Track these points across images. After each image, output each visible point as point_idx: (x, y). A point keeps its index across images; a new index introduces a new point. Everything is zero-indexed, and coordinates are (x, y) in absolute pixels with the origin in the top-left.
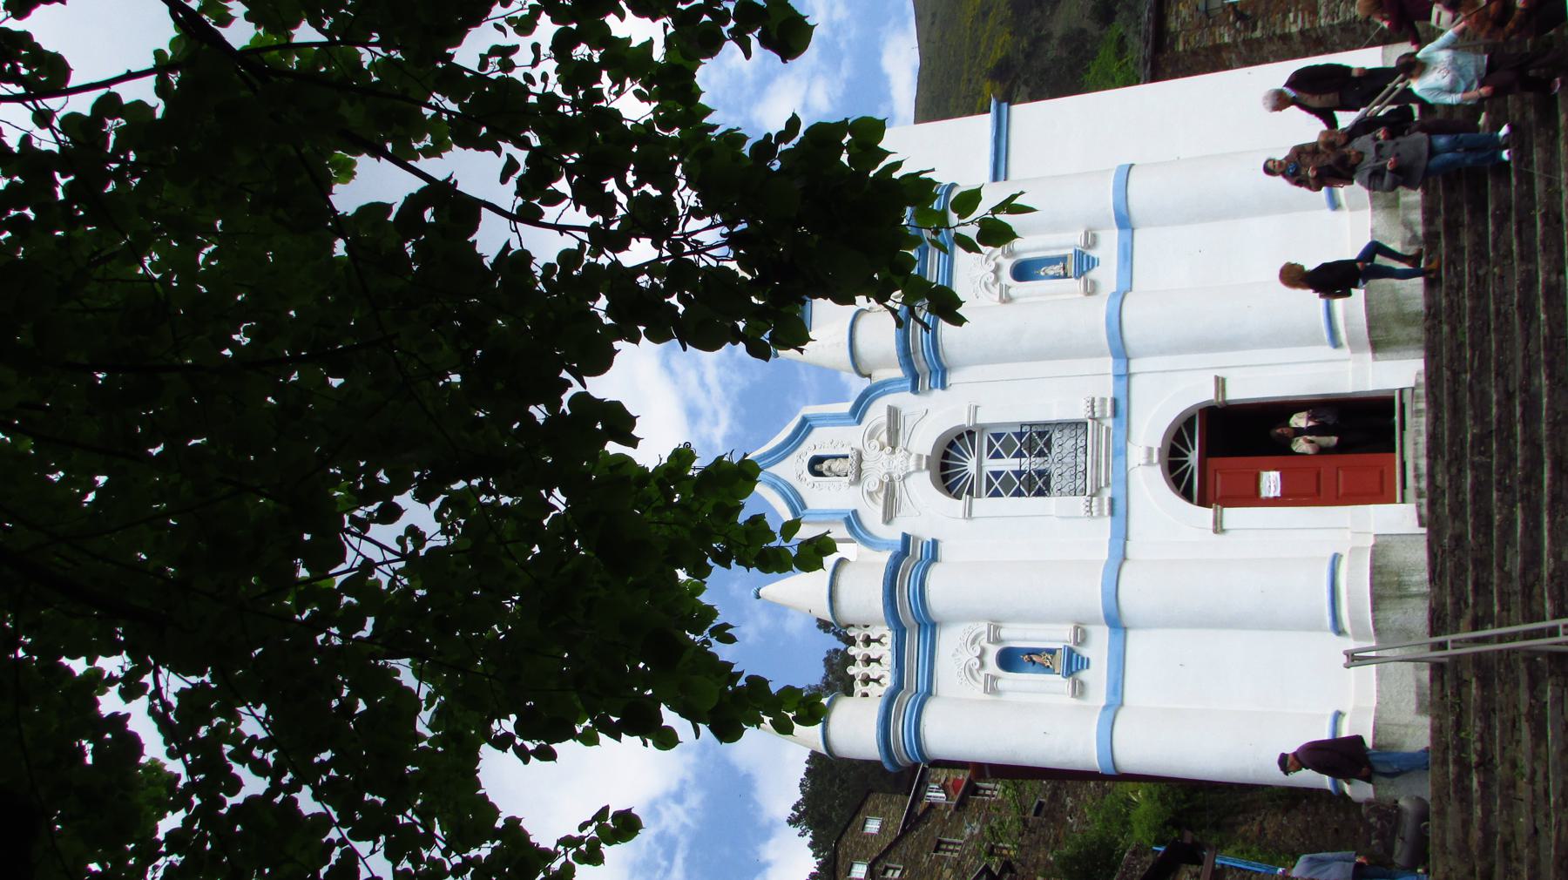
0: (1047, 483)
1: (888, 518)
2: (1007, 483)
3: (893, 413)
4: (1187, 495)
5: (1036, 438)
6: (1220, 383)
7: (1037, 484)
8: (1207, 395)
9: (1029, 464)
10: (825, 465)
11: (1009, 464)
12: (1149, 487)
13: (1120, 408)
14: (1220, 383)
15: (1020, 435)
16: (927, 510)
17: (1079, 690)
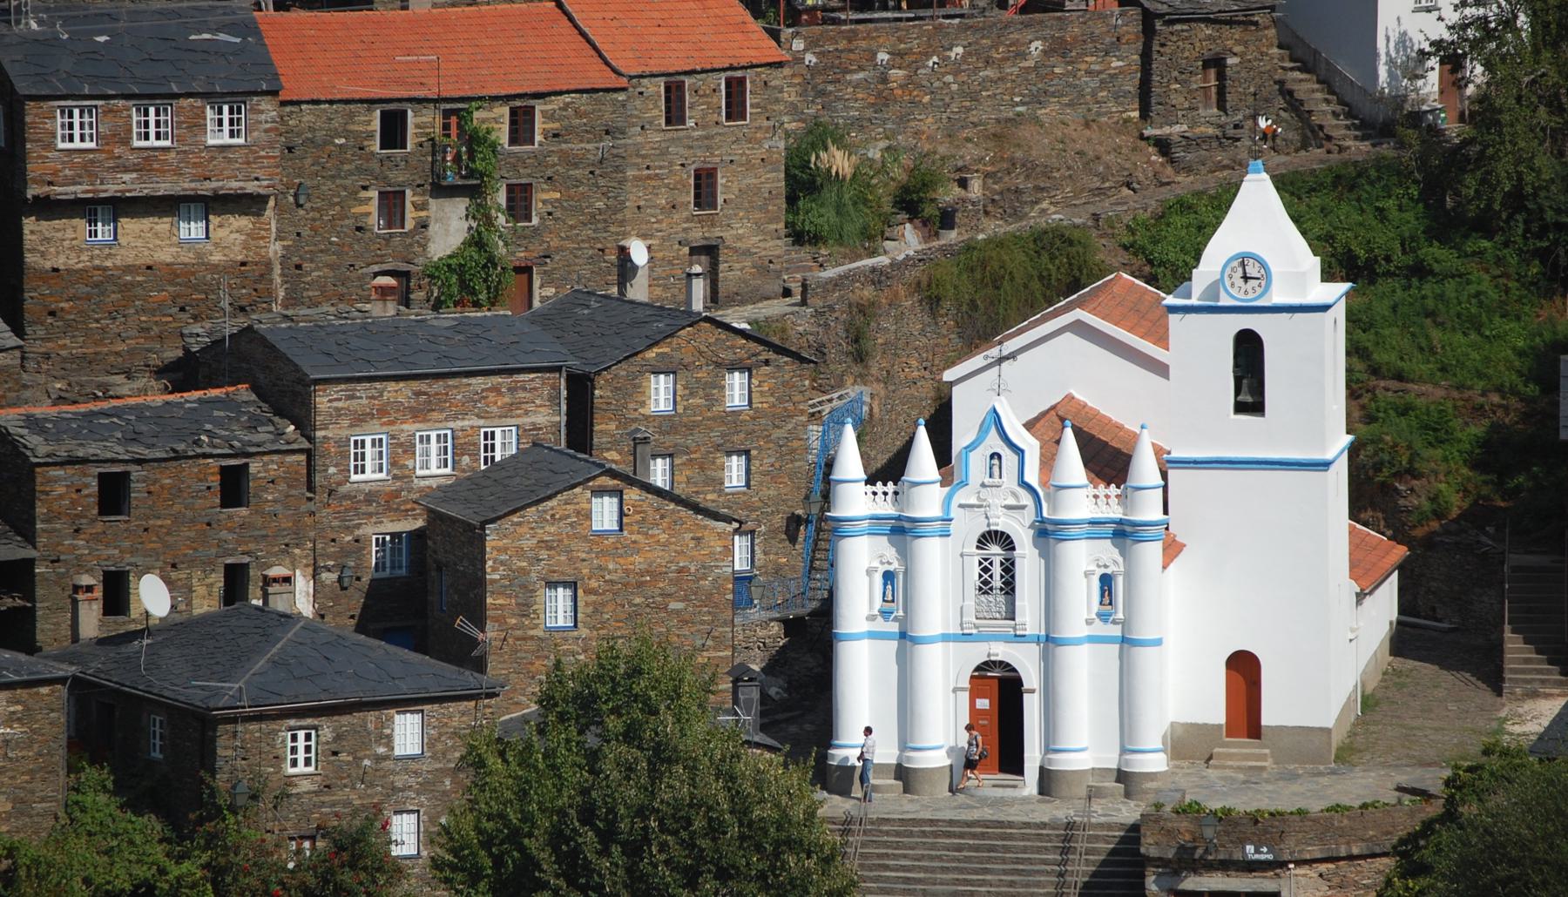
0: (986, 593)
1: (961, 506)
2: (986, 570)
3: (1023, 507)
4: (978, 669)
5: (1009, 587)
6: (1032, 691)
7: (985, 587)
8: (1026, 686)
9: (997, 582)
10: (996, 461)
11: (997, 570)
12: (978, 653)
13: (1020, 638)
14: (1032, 691)
15: (1013, 577)
16: (968, 527)
17: (871, 618)
